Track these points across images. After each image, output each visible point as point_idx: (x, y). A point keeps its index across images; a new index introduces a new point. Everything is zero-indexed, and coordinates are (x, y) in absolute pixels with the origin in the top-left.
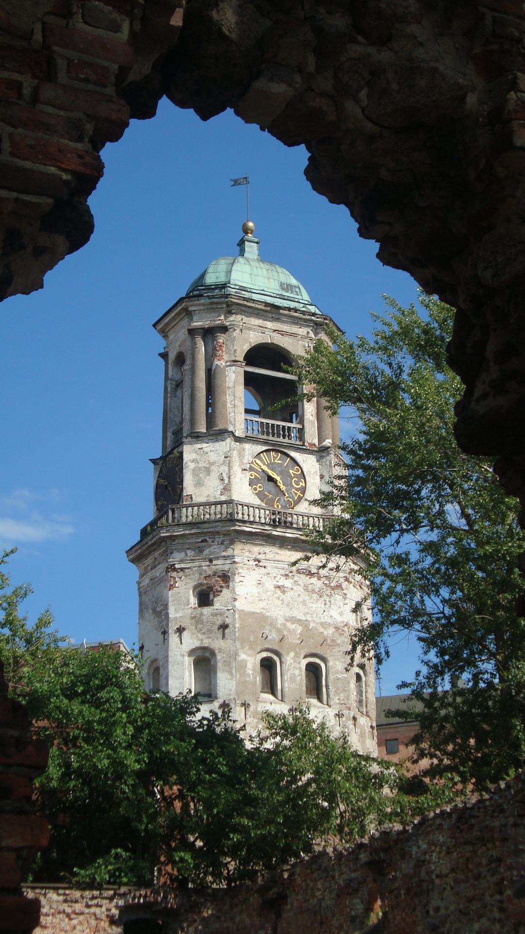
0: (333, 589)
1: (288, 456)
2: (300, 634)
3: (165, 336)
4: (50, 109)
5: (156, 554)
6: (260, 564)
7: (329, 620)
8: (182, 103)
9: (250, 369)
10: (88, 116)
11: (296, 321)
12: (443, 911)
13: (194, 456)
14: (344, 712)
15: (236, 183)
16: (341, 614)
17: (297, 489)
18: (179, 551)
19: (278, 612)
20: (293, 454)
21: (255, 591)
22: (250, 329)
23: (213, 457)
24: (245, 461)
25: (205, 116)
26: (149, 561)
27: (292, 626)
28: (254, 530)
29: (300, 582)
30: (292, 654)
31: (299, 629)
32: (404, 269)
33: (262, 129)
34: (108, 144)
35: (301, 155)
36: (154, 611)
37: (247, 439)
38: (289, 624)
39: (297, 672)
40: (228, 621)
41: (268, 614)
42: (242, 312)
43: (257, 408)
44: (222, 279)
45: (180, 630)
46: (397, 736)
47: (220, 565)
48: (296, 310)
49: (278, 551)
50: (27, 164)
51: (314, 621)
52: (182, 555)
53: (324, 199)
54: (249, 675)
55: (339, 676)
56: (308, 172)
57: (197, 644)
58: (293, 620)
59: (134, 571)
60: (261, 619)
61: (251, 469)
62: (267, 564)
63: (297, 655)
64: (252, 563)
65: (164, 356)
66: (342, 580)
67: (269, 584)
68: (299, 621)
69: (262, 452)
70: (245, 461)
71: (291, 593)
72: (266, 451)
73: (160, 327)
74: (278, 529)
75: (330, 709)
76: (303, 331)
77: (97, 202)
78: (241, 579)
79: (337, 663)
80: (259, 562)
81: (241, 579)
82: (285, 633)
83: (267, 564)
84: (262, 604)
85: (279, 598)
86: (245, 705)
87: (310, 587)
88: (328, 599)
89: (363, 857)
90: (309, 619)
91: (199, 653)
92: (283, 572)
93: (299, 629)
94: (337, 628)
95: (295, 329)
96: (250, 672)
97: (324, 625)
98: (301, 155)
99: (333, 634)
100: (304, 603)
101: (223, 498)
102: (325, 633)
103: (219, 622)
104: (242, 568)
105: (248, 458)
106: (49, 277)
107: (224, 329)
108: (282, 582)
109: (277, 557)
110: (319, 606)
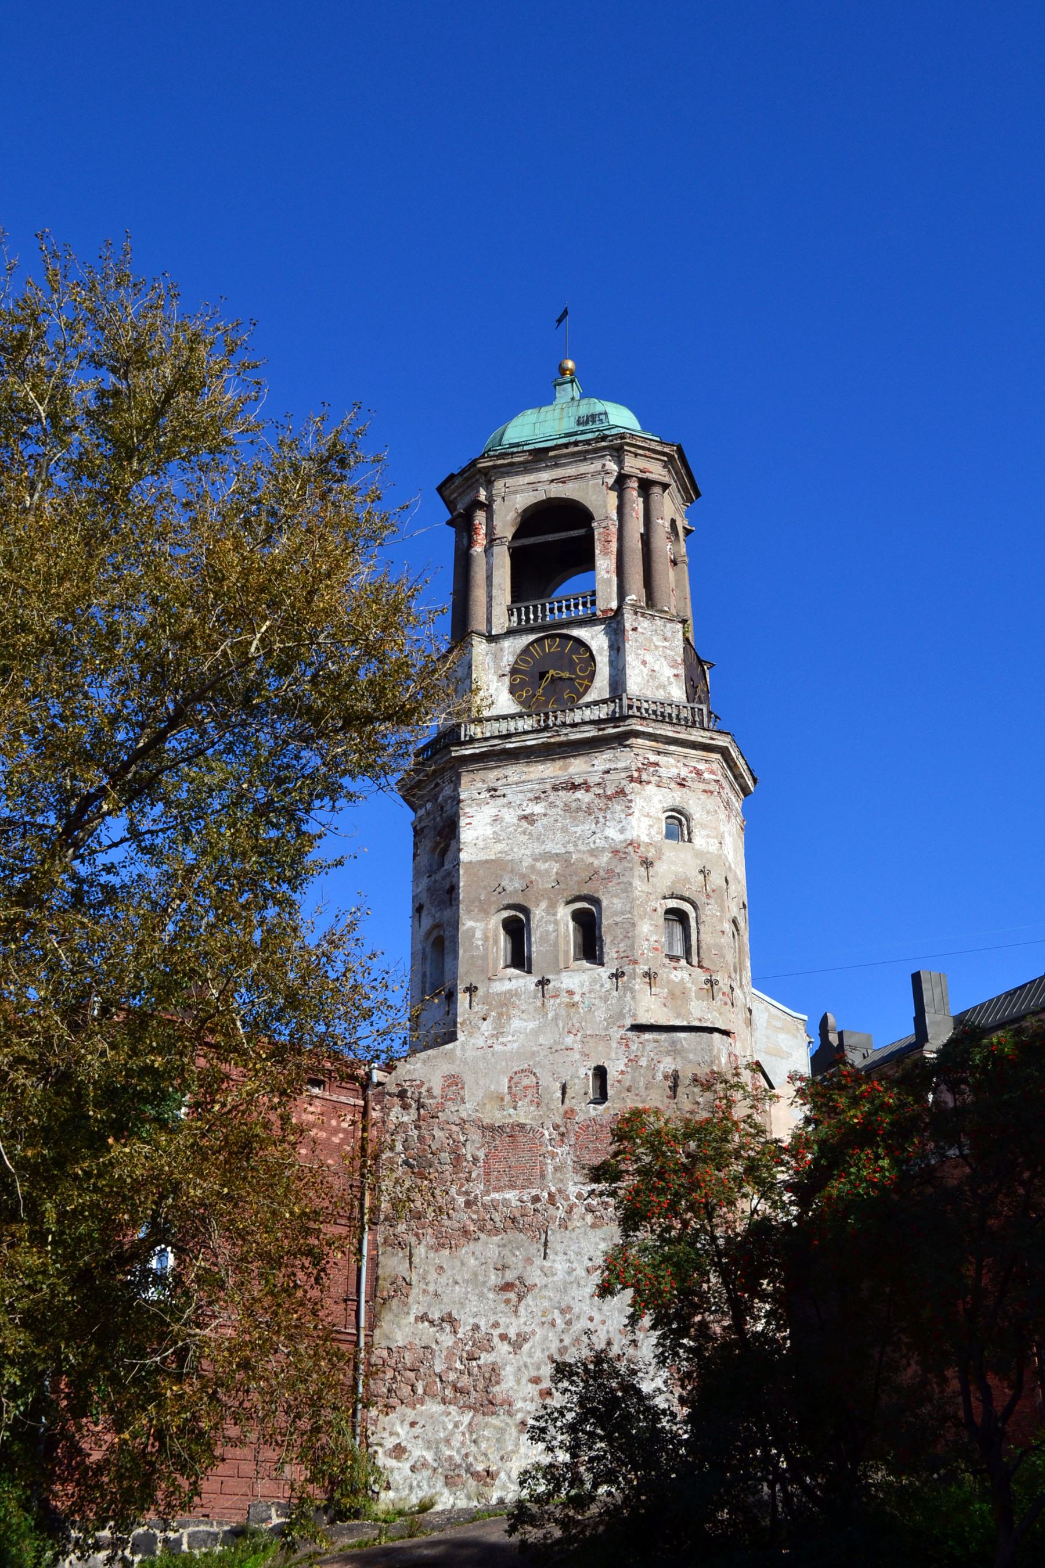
0: (609, 798)
2: (557, 873)
6: (497, 794)
7: (600, 843)
11: (582, 457)
14: (625, 969)
15: (559, 321)
16: (622, 831)
17: (582, 678)
19: (523, 852)
20: (576, 632)
21: (489, 831)
22: (515, 492)
24: (504, 663)
27: (541, 866)
28: (477, 751)
29: (558, 803)
30: (544, 905)
31: (555, 867)
37: (510, 633)
38: (541, 866)
39: (551, 928)
41: (509, 858)
42: (508, 474)
48: (576, 444)
49: (525, 769)
51: (579, 851)
54: (477, 947)
55: (618, 919)
58: (546, 856)
60: (496, 866)
62: (507, 791)
64: (485, 795)
66: (624, 782)
67: (510, 817)
69: (531, 644)
70: (504, 663)
71: (545, 821)
72: (536, 641)
74: (513, 739)
75: (603, 969)
76: (597, 466)
78: (468, 820)
79: (615, 900)
80: (495, 790)
81: (468, 820)
82: (534, 878)
83: (507, 791)
84: (499, 847)
85: (524, 833)
86: (471, 990)
87: (574, 805)
88: (601, 815)
90: (571, 848)
91: (435, 934)
92: (531, 795)
95: (585, 468)
96: (480, 943)
97: (593, 853)
99: (609, 863)
102: (596, 863)
104: (470, 806)
109: (524, 777)
110: (587, 827)
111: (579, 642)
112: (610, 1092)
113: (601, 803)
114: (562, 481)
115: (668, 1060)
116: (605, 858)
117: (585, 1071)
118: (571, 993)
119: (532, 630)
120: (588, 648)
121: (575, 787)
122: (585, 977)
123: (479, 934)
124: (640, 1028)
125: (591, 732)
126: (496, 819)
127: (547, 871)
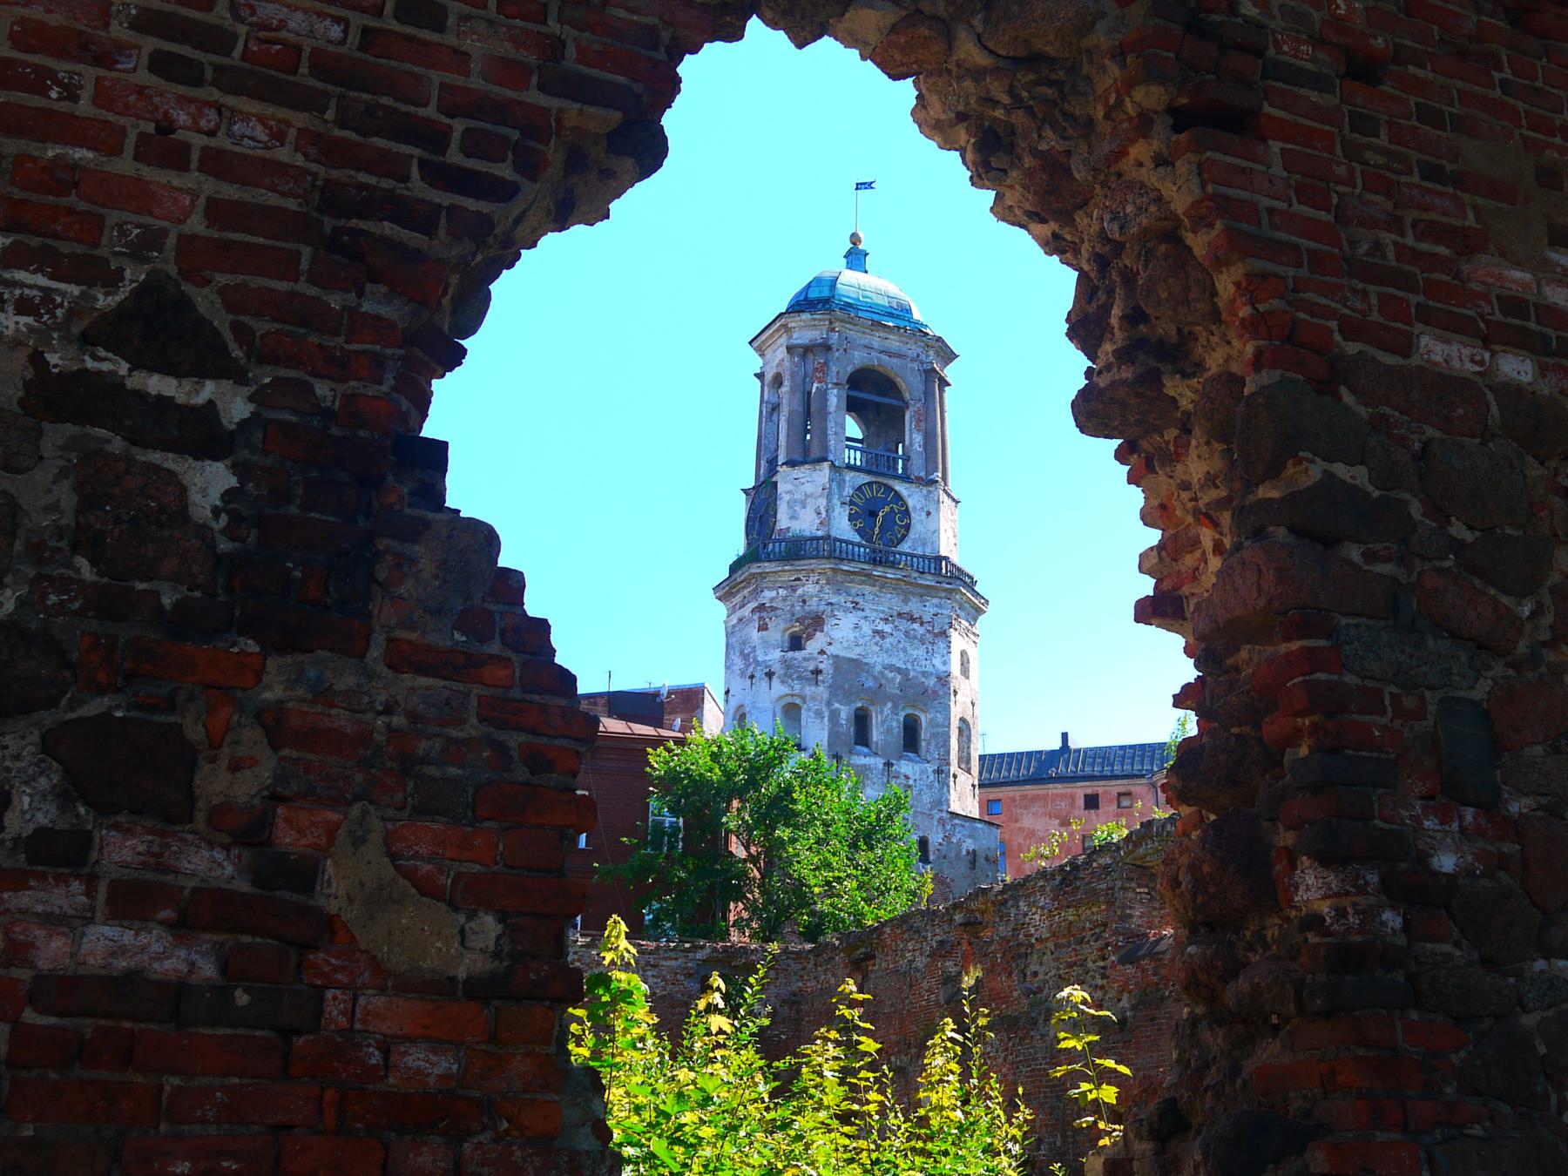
0: (936, 635)
1: (892, 489)
3: (762, 355)
4: (622, 13)
5: (746, 592)
8: (773, 24)
9: (854, 394)
10: (665, 22)
12: (1041, 976)
13: (789, 487)
16: (944, 663)
18: (769, 589)
19: (877, 659)
21: (851, 635)
23: (809, 488)
25: (800, 46)
26: (738, 599)
31: (898, 678)
32: (1021, 226)
33: (863, 58)
34: (687, 57)
35: (906, 91)
36: (742, 653)
40: (821, 666)
43: (860, 436)
44: (826, 293)
45: (770, 675)
46: (1001, 796)
47: (813, 604)
50: (595, 72)
52: (774, 594)
53: (933, 145)
56: (913, 113)
57: (786, 690)
58: (892, 668)
59: (721, 609)
60: (857, 665)
61: (852, 503)
62: (868, 606)
63: (895, 706)
64: (850, 605)
65: (760, 376)
67: (867, 628)
68: (899, 670)
73: (756, 344)
77: (670, 121)
83: (868, 606)
84: (859, 650)
86: (838, 757)
89: (958, 918)
91: (789, 699)
93: (898, 678)
94: (939, 678)
97: (925, 674)
98: (906, 91)
100: (905, 650)
101: (820, 533)
103: (811, 668)
105: (848, 491)
106: (614, 206)
107: (826, 347)
108: (881, 626)
110: (918, 652)
111: (898, 497)
112: (932, 858)
113: (929, 637)
114: (891, 354)
115: (970, 841)
116: (932, 682)
117: (915, 838)
118: (907, 777)
119: (869, 472)
120: (905, 504)
121: (912, 619)
122: (917, 767)
123: (843, 715)
124: (955, 815)
125: (929, 581)
126: (857, 627)
127: (893, 679)
